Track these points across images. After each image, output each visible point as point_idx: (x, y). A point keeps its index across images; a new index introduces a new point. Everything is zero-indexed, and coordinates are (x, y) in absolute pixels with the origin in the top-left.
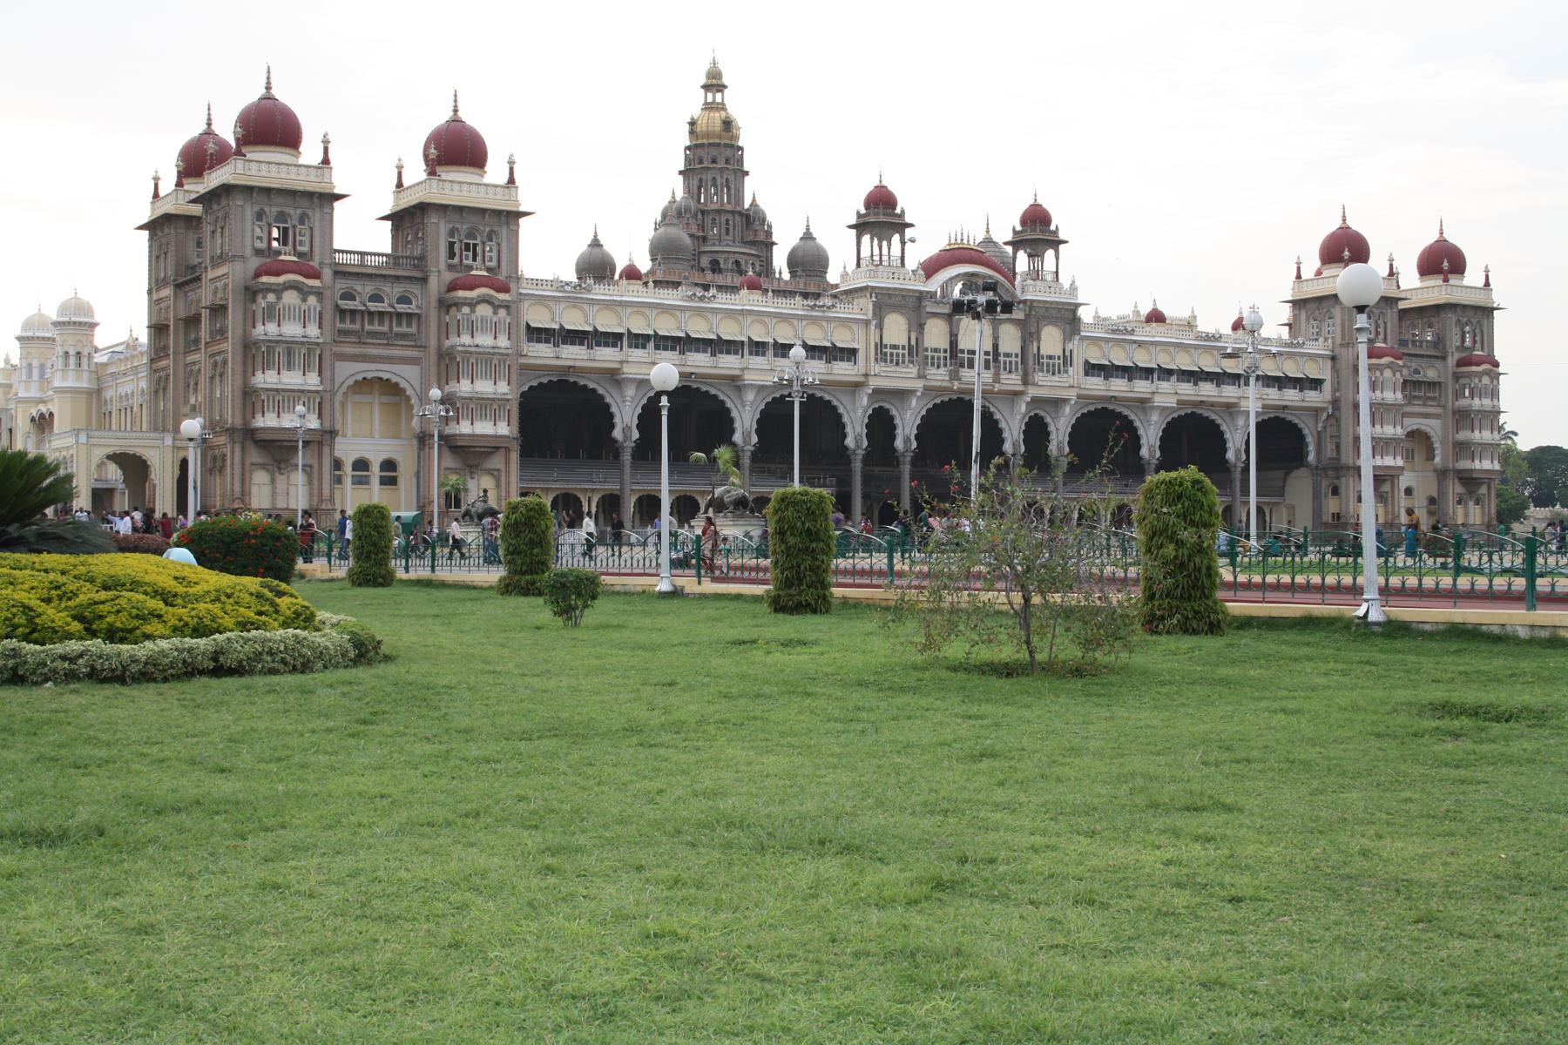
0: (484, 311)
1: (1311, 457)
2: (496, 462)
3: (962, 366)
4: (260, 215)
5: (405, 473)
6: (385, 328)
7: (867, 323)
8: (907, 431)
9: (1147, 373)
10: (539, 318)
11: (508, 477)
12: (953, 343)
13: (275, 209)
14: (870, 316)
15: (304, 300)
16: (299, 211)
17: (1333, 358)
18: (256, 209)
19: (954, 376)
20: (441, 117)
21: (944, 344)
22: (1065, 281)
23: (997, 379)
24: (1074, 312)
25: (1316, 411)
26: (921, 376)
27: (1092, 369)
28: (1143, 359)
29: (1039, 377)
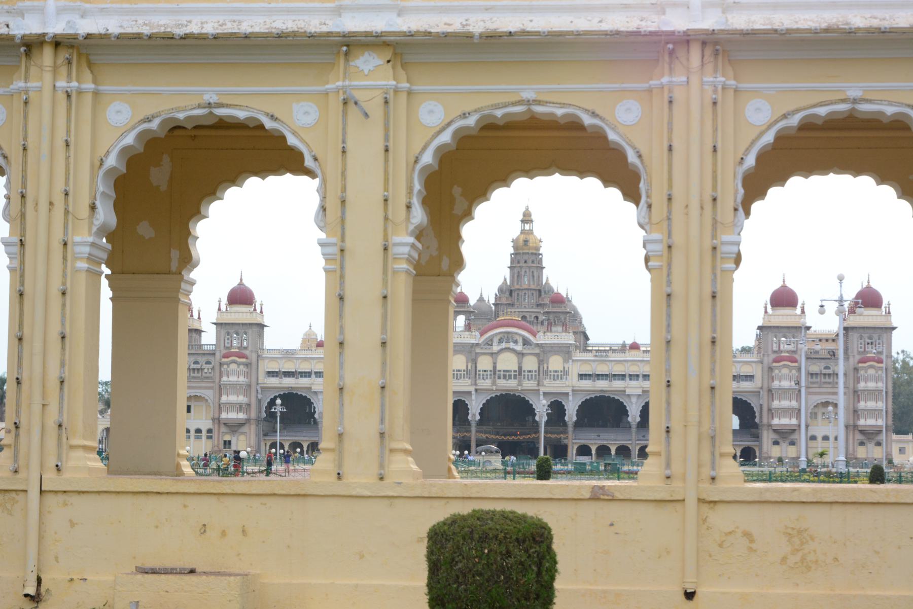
0: (233, 366)
1: (757, 420)
2: (245, 429)
3: (499, 378)
8: (474, 411)
9: (623, 377)
10: (274, 367)
12: (495, 367)
17: (761, 362)
19: (494, 383)
20: (234, 283)
21: (489, 367)
23: (520, 384)
25: (757, 393)
28: (618, 369)
29: (546, 382)
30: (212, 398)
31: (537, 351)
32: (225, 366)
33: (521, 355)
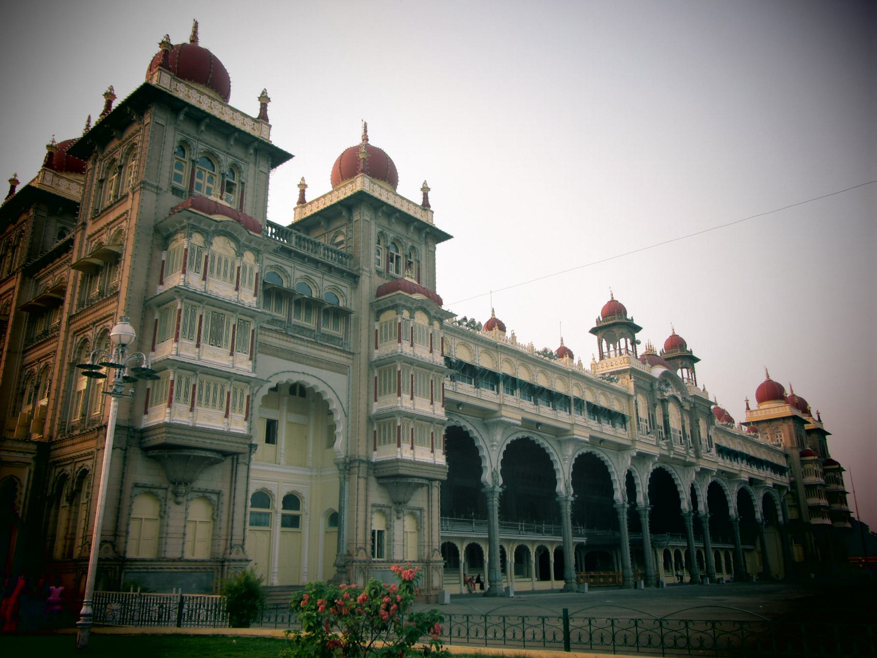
1: (781, 519)
2: (418, 499)
4: (183, 147)
5: (313, 515)
6: (312, 325)
7: (629, 397)
11: (430, 518)
13: (202, 147)
14: (632, 392)
15: (239, 254)
16: (230, 160)
18: (179, 137)
22: (700, 386)
24: (710, 409)
26: (658, 445)
27: (722, 451)
30: (343, 398)
31: (687, 408)
32: (406, 314)
33: (681, 407)
